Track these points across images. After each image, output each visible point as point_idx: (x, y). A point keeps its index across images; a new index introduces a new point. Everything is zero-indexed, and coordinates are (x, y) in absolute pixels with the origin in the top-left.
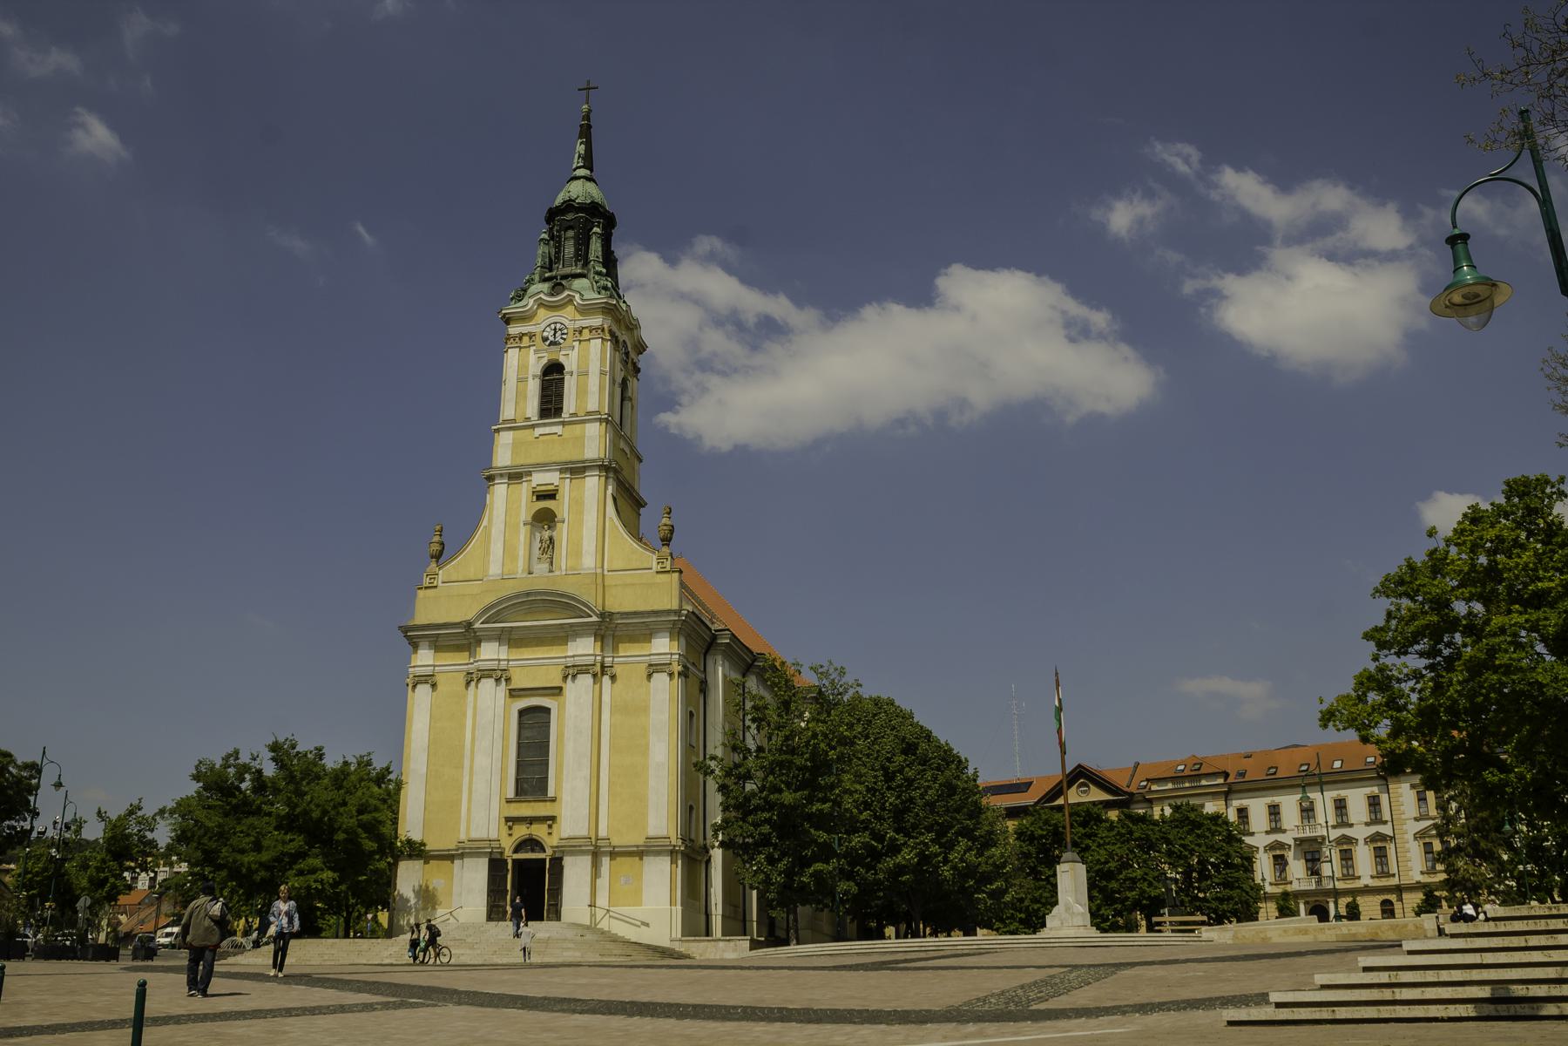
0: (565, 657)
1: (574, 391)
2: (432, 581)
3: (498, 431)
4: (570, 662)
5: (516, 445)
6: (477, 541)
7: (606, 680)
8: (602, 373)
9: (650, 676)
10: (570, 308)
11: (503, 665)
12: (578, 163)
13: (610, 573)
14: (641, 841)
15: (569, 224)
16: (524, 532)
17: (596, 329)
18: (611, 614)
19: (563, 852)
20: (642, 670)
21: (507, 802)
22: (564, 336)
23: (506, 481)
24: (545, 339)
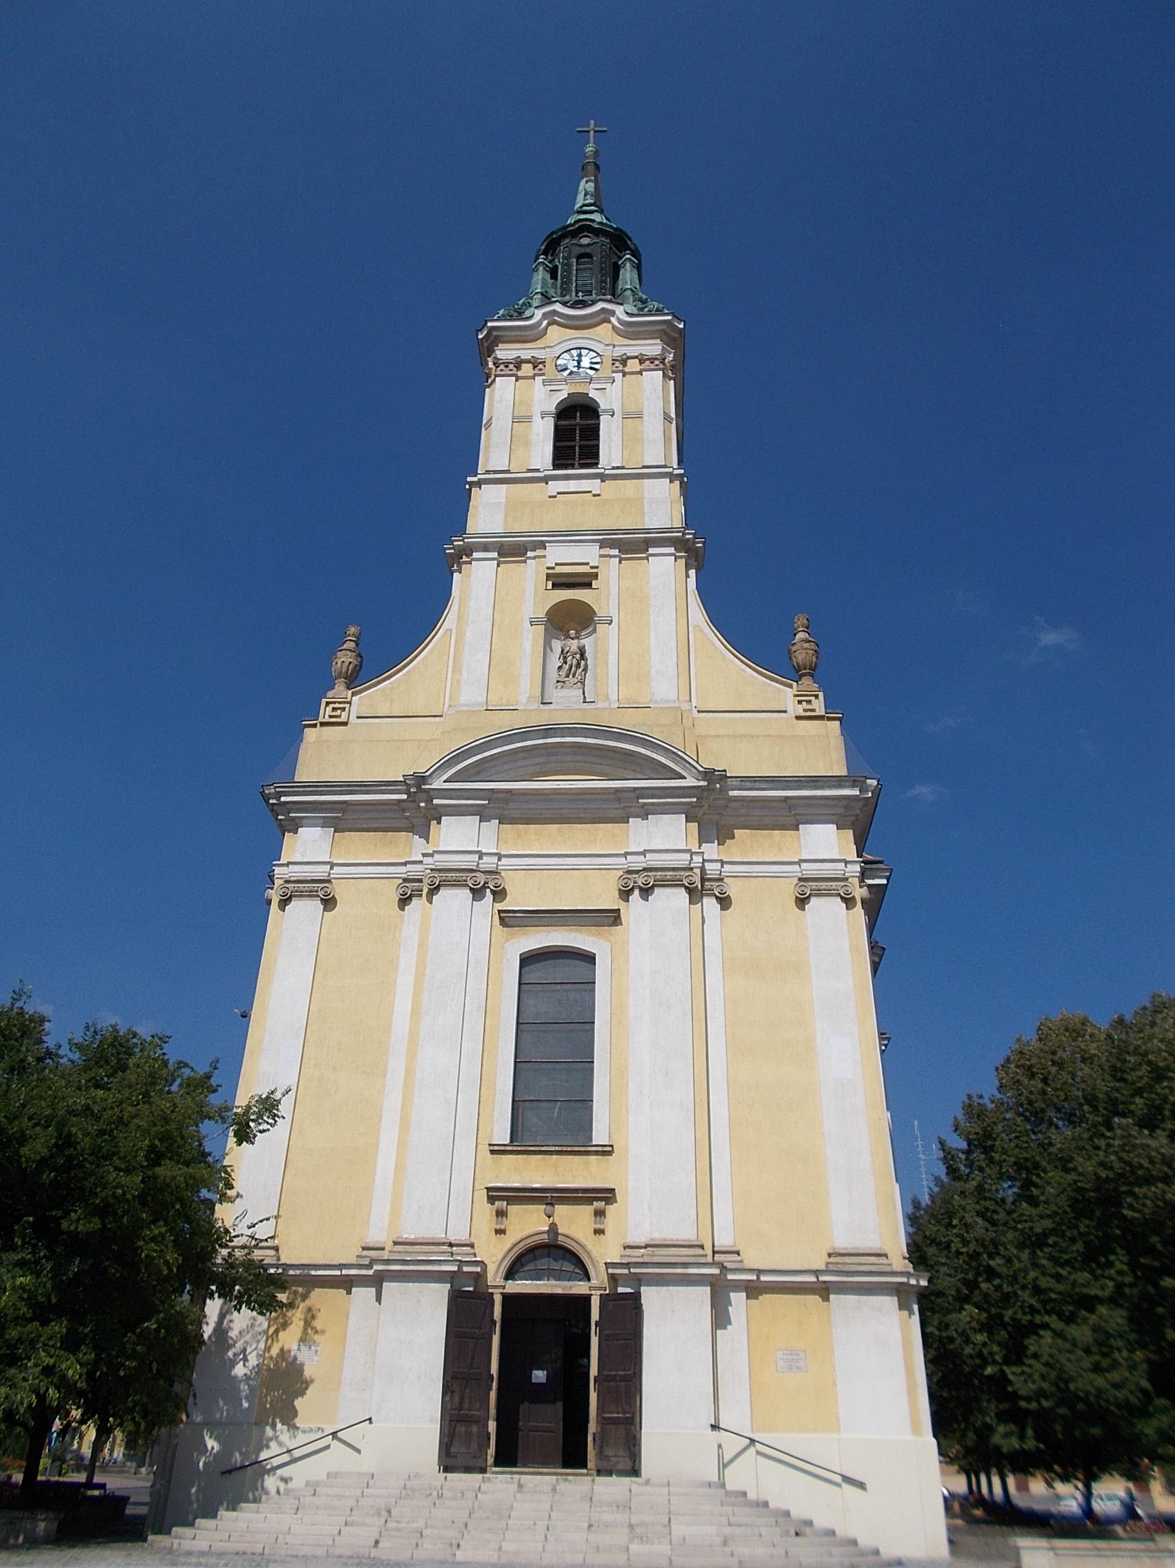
0: (626, 854)
1: (617, 437)
2: (338, 712)
3: (479, 484)
4: (638, 862)
5: (511, 507)
6: (431, 651)
7: (710, 904)
8: (667, 417)
9: (802, 902)
10: (603, 331)
11: (488, 863)
12: (585, 200)
13: (702, 715)
14: (819, 1263)
15: (583, 250)
16: (532, 638)
17: (652, 360)
18: (723, 777)
19: (639, 1280)
20: (789, 889)
21: (492, 1152)
23: (495, 555)
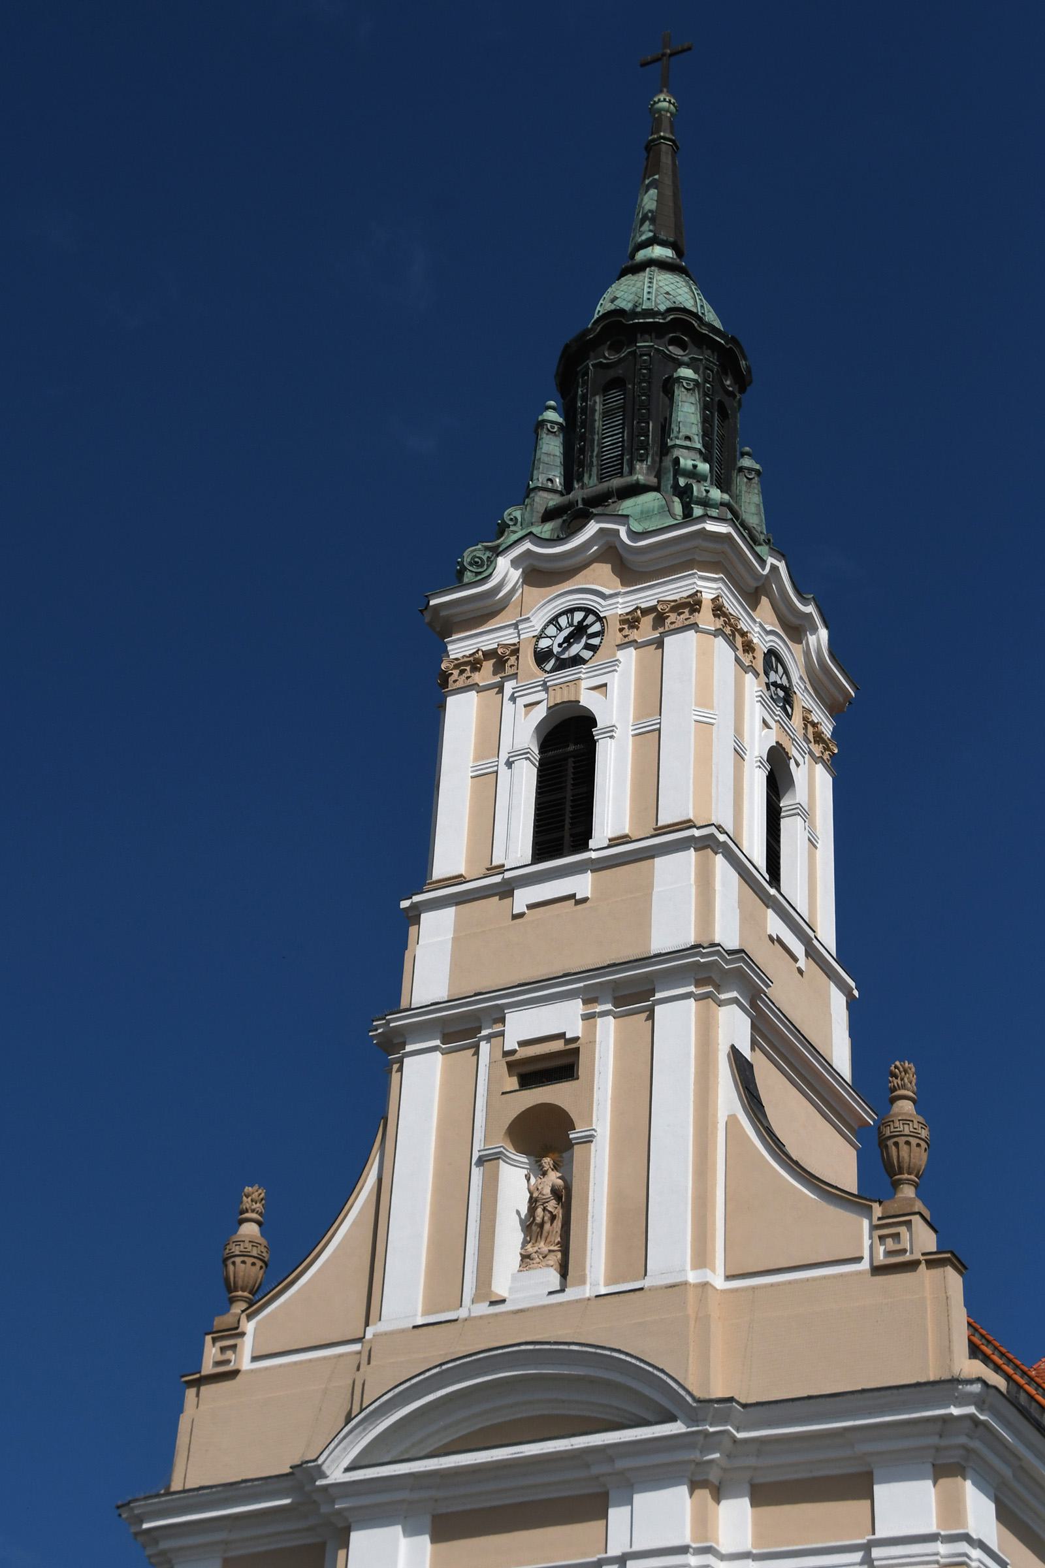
2: (229, 1355)
15: (612, 373)
22: (595, 641)
23: (437, 1042)
24: (542, 657)
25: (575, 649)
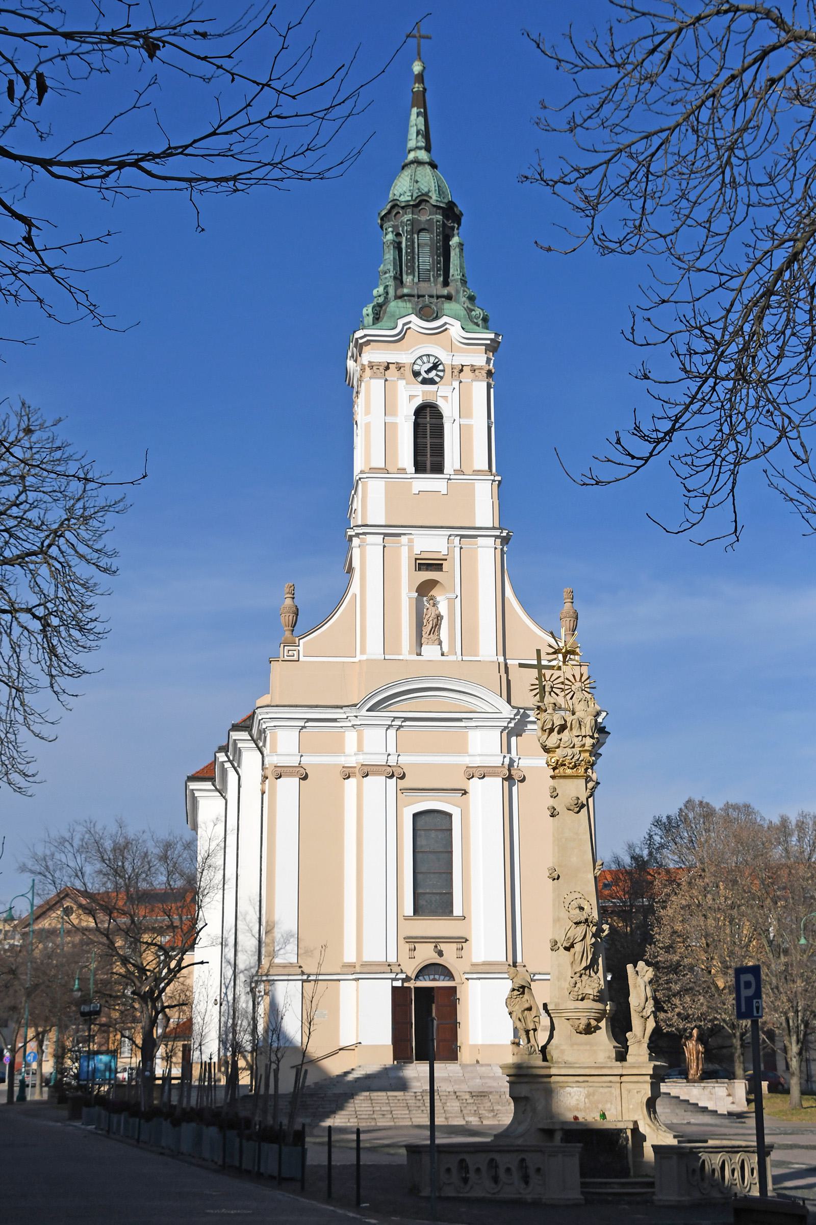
22: (441, 374)
24: (416, 374)
25: (433, 374)
